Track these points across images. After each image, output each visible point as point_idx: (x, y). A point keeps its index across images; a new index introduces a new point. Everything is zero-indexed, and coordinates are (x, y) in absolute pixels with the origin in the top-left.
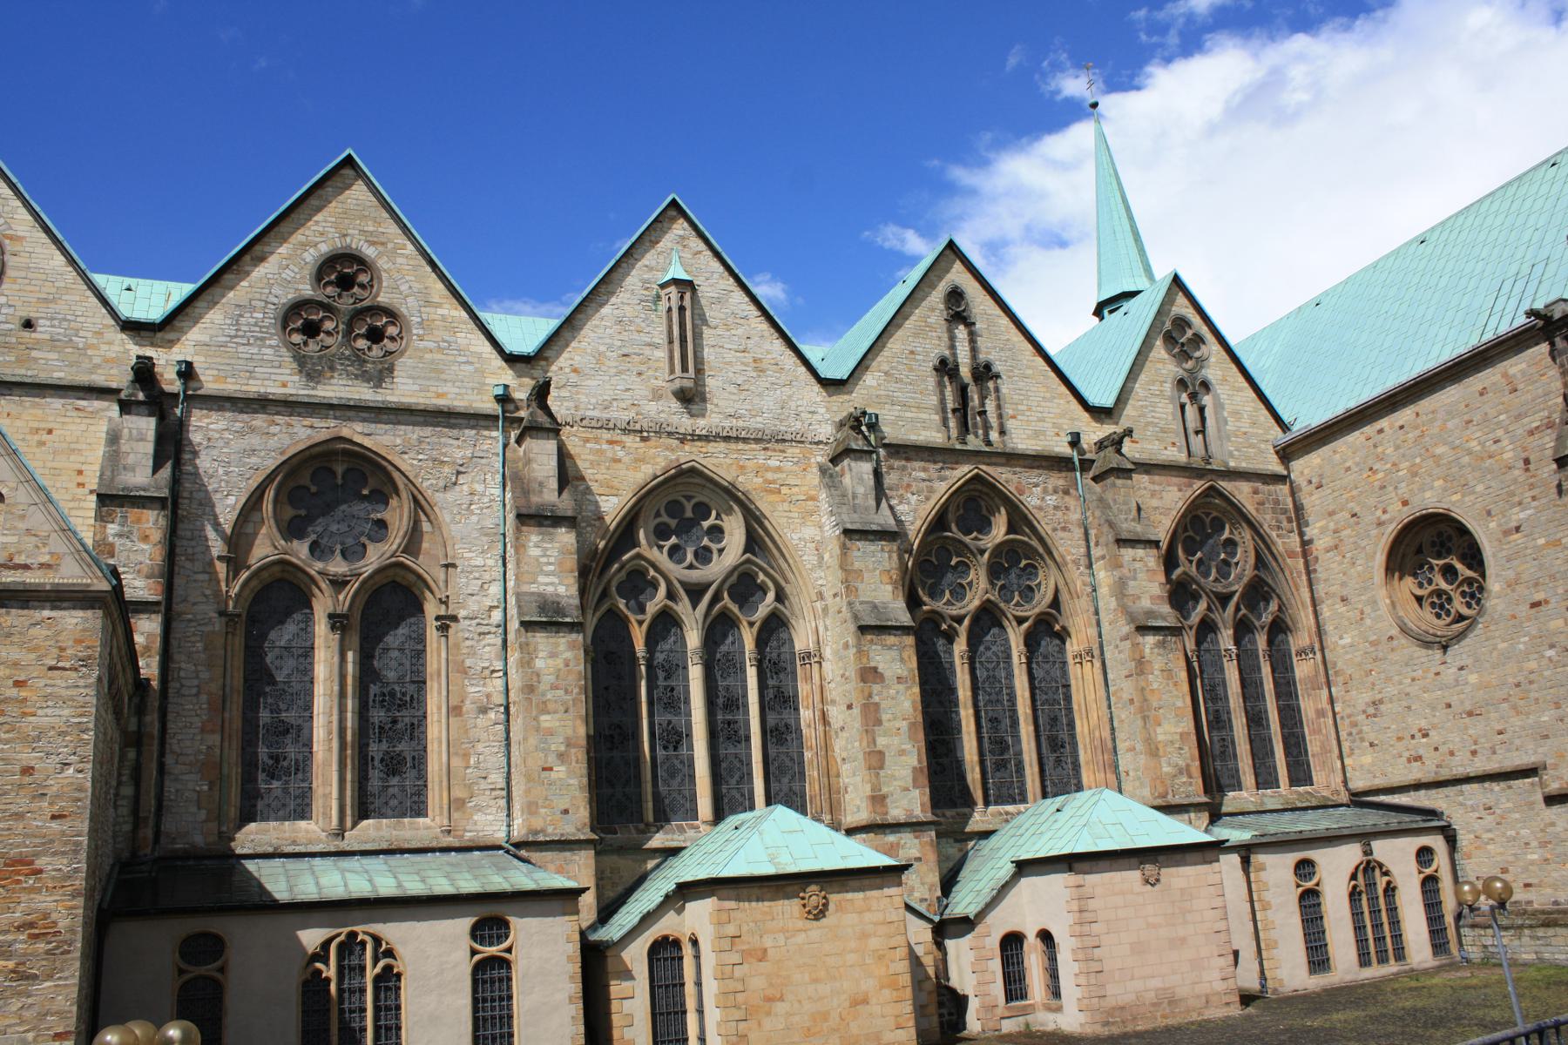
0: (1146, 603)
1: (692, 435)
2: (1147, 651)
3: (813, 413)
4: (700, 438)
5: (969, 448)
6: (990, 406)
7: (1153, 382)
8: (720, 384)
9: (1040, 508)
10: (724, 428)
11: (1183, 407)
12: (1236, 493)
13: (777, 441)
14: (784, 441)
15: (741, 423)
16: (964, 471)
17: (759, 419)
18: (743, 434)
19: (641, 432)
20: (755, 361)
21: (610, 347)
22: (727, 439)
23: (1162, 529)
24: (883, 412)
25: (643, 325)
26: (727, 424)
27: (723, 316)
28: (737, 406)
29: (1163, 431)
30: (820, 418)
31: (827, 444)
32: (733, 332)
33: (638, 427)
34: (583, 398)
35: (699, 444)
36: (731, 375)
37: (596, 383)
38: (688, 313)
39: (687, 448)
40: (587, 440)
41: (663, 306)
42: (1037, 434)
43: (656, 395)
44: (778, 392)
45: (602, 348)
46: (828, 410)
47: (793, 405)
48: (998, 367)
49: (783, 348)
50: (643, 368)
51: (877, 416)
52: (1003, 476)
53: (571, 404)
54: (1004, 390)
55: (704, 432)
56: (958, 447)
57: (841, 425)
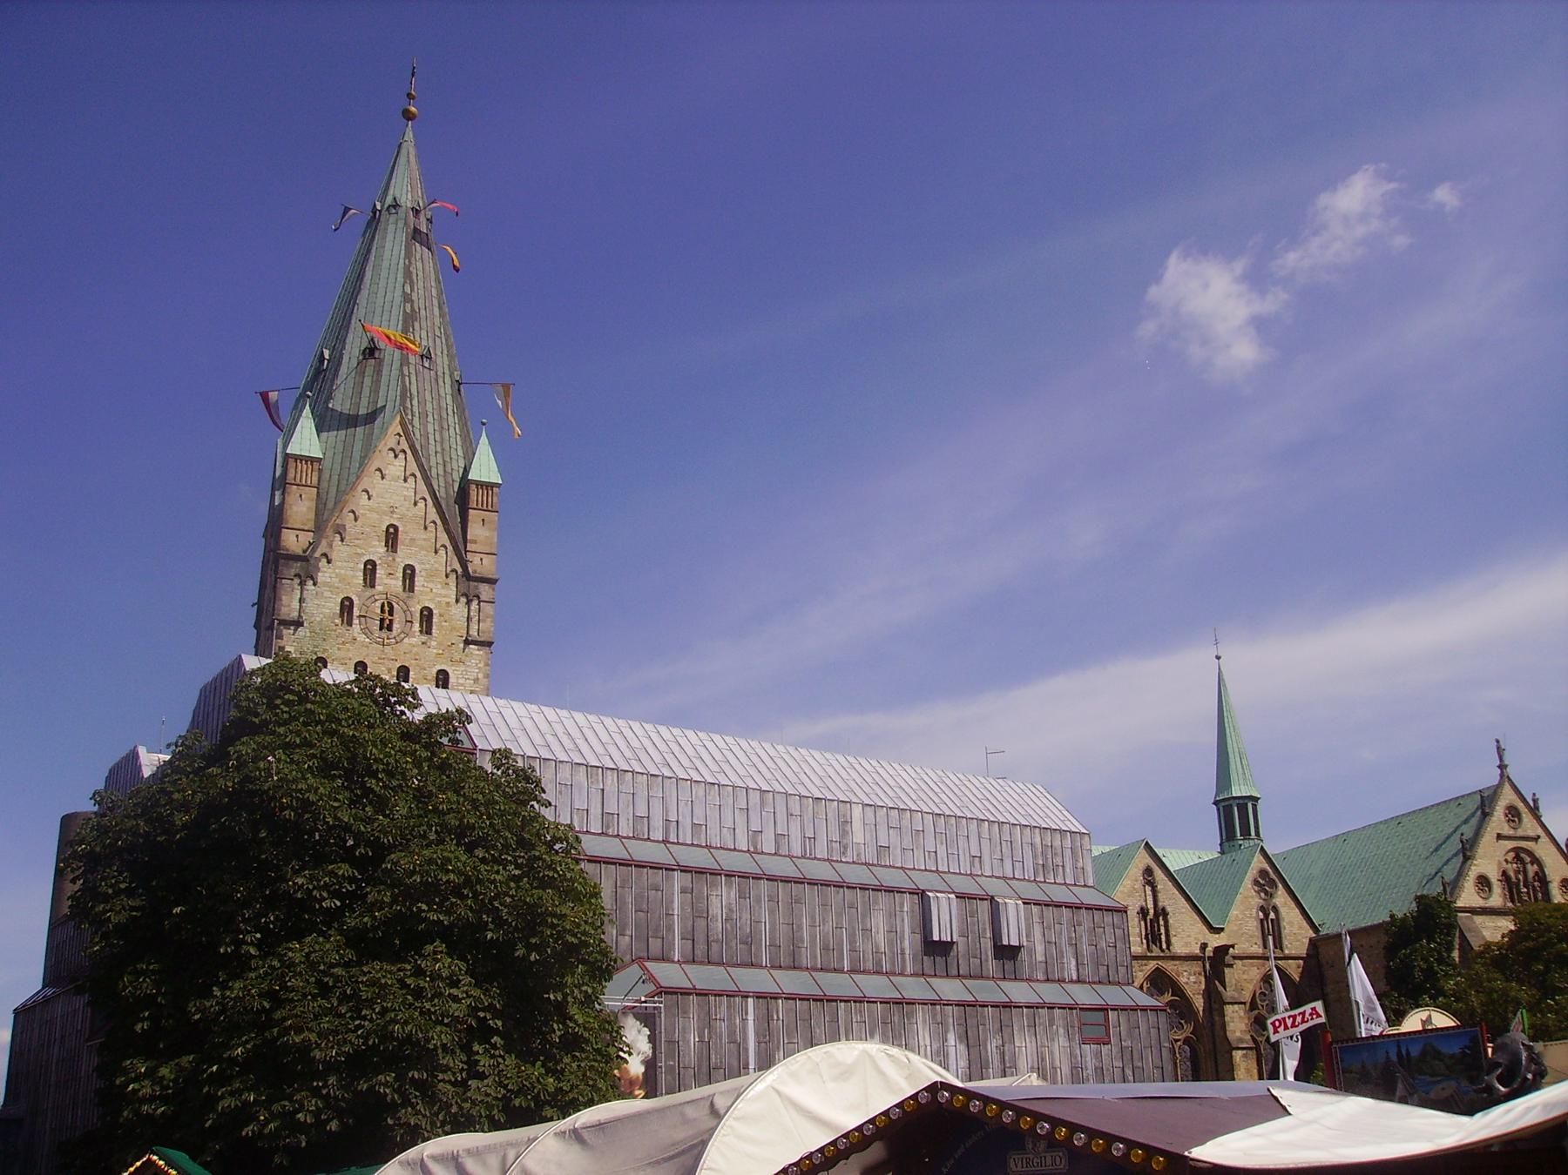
0: (1238, 1034)
2: (1238, 1060)
5: (1153, 954)
6: (1163, 931)
7: (1246, 910)
9: (1187, 983)
11: (1261, 920)
12: (1288, 968)
16: (1152, 965)
23: (1247, 996)
29: (1251, 937)
42: (1187, 944)
48: (1169, 909)
52: (1169, 967)
54: (1171, 921)
56: (1149, 954)
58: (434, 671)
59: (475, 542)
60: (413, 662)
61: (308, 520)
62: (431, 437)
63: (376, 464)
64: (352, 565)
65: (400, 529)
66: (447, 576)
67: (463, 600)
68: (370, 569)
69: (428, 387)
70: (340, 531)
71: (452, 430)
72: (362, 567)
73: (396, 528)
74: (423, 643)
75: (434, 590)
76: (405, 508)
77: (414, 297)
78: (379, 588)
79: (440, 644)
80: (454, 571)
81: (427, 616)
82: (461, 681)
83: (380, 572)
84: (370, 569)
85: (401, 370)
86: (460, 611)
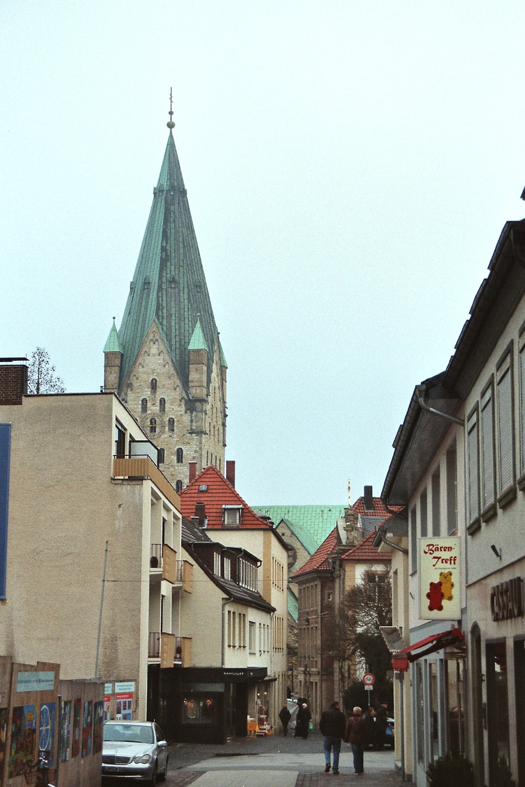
58: (176, 449)
59: (192, 381)
60: (166, 446)
61: (115, 383)
62: (173, 328)
63: (144, 350)
64: (136, 402)
65: (158, 380)
66: (180, 401)
67: (188, 412)
68: (144, 401)
69: (173, 299)
70: (130, 385)
71: (187, 320)
72: (141, 402)
73: (156, 381)
74: (170, 436)
75: (174, 409)
76: (161, 370)
77: (168, 248)
78: (149, 412)
79: (178, 435)
80: (183, 398)
81: (171, 422)
82: (188, 453)
83: (149, 404)
84: (144, 401)
85: (158, 294)
86: (186, 418)
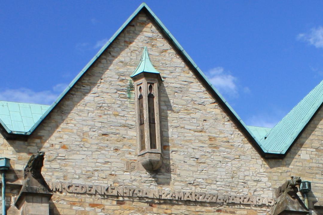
1: (159, 199)
3: (258, 181)
4: (166, 202)
8: (182, 158)
10: (185, 194)
13: (228, 204)
14: (234, 204)
15: (198, 190)
17: (214, 186)
18: (201, 199)
19: (117, 197)
20: (210, 139)
21: (92, 127)
22: (187, 202)
24: (315, 180)
25: (119, 109)
26: (188, 190)
27: (185, 103)
28: (195, 176)
30: (263, 185)
31: (268, 206)
32: (193, 115)
33: (115, 193)
34: (70, 169)
35: (165, 206)
36: (190, 150)
37: (81, 157)
38: (156, 100)
39: (155, 210)
40: (73, 204)
41: (135, 94)
43: (130, 167)
44: (229, 164)
45: (86, 129)
46: (270, 179)
47: (241, 175)
49: (233, 129)
50: (119, 145)
51: (309, 184)
53: (60, 174)
55: (169, 197)
57: (280, 191)
